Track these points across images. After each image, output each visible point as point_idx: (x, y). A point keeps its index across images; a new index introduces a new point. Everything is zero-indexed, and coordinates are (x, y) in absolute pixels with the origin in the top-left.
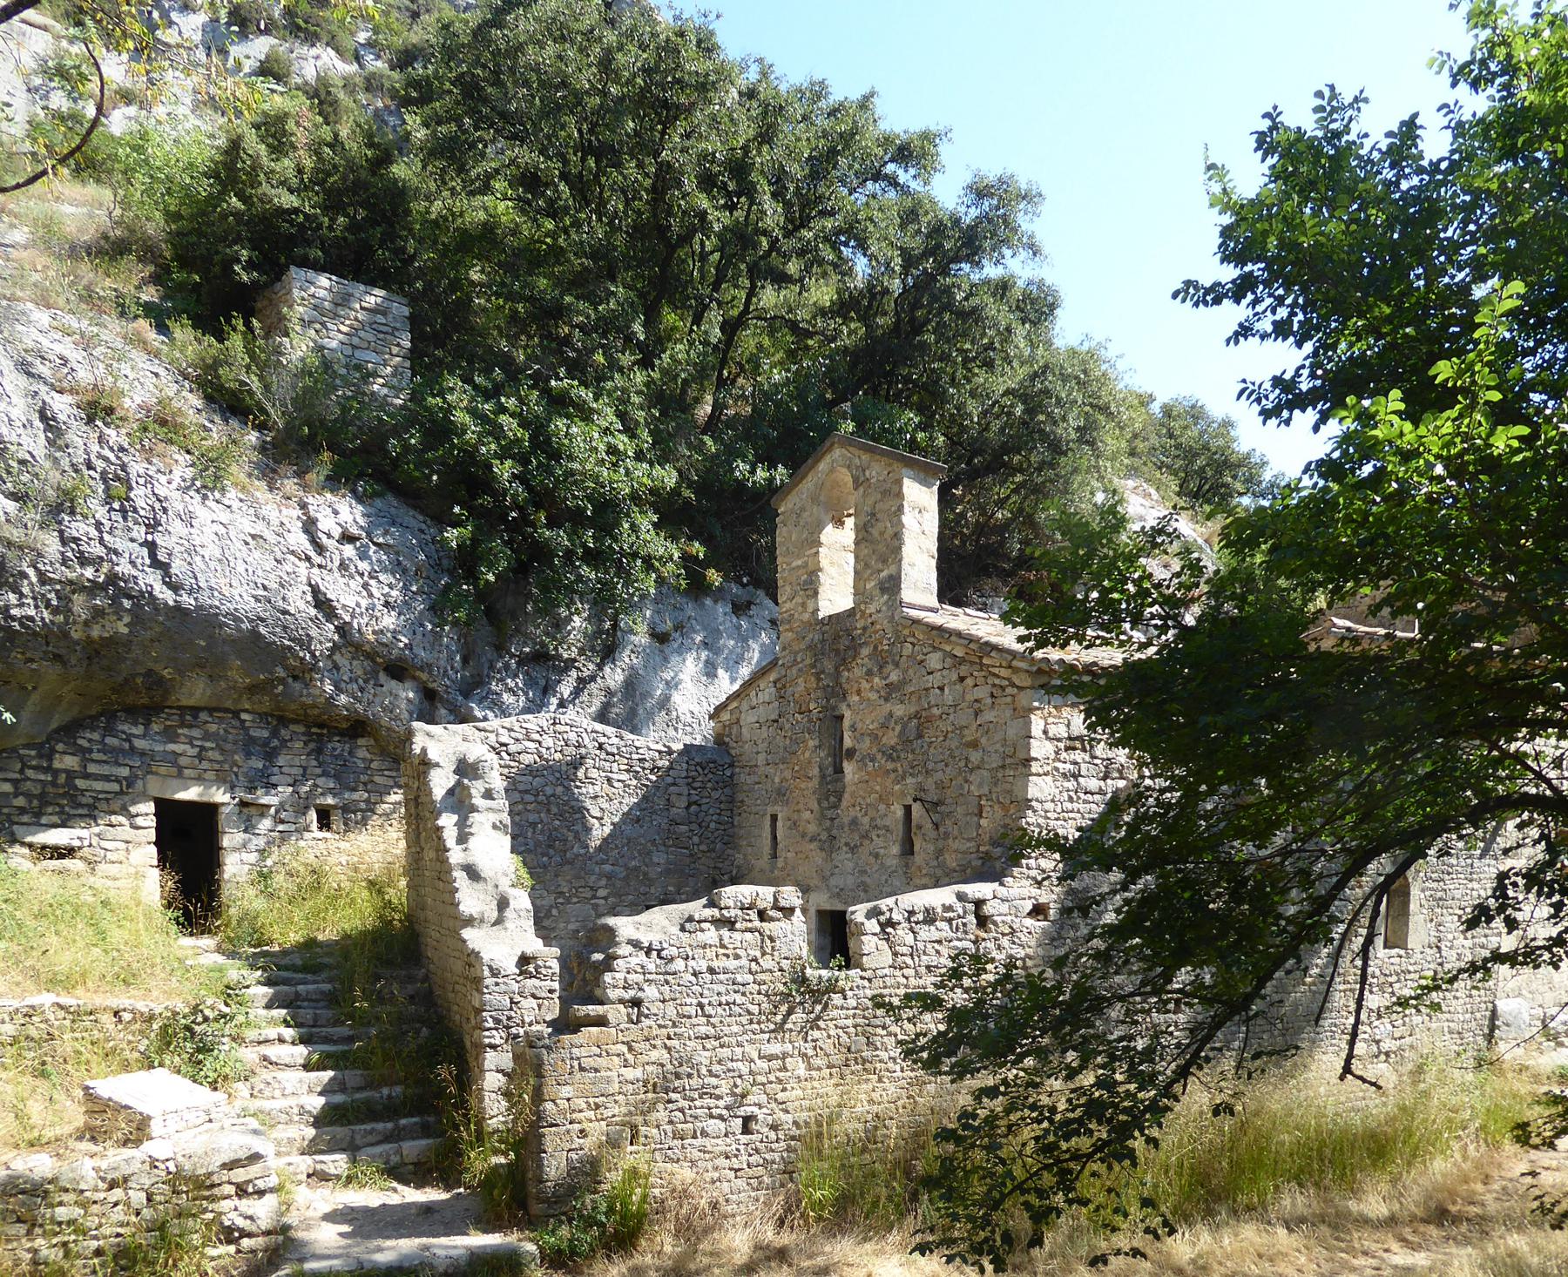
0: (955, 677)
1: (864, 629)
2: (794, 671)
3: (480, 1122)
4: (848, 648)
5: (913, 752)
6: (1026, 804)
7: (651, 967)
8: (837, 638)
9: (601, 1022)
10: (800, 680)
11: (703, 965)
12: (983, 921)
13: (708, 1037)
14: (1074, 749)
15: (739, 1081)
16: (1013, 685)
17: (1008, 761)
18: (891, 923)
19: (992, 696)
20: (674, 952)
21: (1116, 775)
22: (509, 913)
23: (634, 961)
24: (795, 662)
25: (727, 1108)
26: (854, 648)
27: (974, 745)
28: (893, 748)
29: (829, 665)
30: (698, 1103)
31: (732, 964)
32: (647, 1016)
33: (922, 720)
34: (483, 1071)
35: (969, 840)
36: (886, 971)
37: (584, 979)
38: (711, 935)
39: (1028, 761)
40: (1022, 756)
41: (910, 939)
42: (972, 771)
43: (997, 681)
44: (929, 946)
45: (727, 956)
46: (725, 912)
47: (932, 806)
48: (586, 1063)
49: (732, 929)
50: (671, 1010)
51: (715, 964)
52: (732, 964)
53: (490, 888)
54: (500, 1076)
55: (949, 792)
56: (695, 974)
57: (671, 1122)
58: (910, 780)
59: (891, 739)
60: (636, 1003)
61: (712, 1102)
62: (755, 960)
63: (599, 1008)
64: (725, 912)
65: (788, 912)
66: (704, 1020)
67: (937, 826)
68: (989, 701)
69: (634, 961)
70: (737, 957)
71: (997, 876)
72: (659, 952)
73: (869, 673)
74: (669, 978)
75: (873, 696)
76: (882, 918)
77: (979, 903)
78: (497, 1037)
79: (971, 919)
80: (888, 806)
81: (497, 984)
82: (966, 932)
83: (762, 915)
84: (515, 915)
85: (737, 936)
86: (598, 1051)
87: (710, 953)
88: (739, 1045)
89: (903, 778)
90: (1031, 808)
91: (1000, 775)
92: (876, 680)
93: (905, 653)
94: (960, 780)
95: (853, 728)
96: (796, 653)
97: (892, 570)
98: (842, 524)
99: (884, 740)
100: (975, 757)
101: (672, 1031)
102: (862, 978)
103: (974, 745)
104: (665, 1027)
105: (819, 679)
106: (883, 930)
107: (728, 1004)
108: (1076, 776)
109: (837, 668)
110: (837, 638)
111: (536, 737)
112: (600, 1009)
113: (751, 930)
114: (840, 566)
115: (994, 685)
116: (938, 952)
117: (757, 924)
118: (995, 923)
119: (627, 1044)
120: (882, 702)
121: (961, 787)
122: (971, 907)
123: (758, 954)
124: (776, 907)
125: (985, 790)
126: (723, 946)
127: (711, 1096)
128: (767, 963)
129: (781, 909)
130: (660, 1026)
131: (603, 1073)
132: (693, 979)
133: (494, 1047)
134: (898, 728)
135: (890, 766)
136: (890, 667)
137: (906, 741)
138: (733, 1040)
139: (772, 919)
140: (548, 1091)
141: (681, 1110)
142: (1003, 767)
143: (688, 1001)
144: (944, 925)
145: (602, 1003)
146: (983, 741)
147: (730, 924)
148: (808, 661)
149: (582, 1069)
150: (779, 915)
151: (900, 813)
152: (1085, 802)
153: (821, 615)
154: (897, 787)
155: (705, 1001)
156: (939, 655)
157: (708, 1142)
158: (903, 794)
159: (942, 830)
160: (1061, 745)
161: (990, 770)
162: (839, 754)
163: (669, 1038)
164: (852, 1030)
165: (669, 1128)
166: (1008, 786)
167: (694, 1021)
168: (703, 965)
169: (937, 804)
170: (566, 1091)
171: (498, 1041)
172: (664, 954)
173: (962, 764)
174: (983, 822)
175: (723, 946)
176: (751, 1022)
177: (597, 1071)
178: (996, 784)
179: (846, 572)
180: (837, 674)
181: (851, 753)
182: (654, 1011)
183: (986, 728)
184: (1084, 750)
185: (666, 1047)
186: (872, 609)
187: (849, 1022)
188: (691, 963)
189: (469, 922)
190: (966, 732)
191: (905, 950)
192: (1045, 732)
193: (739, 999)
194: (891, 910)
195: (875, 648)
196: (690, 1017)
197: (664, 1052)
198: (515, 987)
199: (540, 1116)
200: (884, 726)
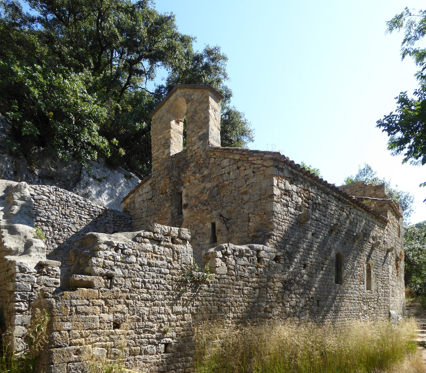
0: (235, 167)
1: (192, 156)
2: (159, 178)
3: (10, 354)
4: (184, 165)
5: (216, 200)
6: (272, 213)
7: (119, 257)
8: (179, 162)
9: (90, 285)
10: (162, 181)
11: (146, 261)
12: (260, 259)
13: (147, 300)
14: (286, 195)
15: (163, 324)
16: (264, 166)
17: (262, 197)
18: (225, 254)
19: (253, 172)
20: (131, 251)
21: (298, 209)
22: (32, 249)
23: (109, 253)
24: (160, 175)
25: (157, 339)
26: (187, 164)
27: (246, 193)
28: (206, 201)
29: (175, 173)
30: (142, 335)
31: (159, 262)
32: (116, 285)
33: (220, 187)
34: (13, 326)
35: (244, 232)
36: (225, 276)
37: (79, 264)
38: (149, 246)
39: (273, 195)
40: (270, 193)
41: (233, 262)
42: (244, 204)
43: (256, 166)
44: (241, 267)
45: (157, 258)
46: (156, 235)
47: (225, 221)
48: (81, 309)
49: (159, 245)
50: (129, 284)
51: (151, 261)
52: (159, 262)
53: (22, 237)
54: (24, 328)
55: (233, 214)
56: (141, 265)
57: (128, 345)
58: (214, 212)
59: (205, 197)
60: (110, 277)
61: (150, 335)
62: (170, 262)
63: (88, 277)
64: (156, 235)
65: (184, 241)
66: (146, 290)
67: (228, 229)
68: (252, 174)
69: (109, 253)
70: (162, 259)
71: (263, 243)
72: (123, 250)
73: (194, 173)
74: (128, 265)
75: (196, 182)
76: (223, 251)
77: (258, 251)
78: (23, 306)
79: (255, 257)
80: (204, 224)
81: (24, 277)
82: (254, 263)
83: (173, 240)
84: (36, 250)
85: (162, 248)
86: (88, 302)
87: (149, 255)
88: (163, 305)
89: (211, 212)
90: (274, 214)
91: (258, 203)
92: (198, 175)
93: (211, 162)
94: (239, 208)
95: (187, 196)
96: (161, 171)
97: (205, 131)
98: (179, 123)
99: (201, 198)
100: (246, 197)
101: (129, 295)
102: (216, 278)
103: (246, 193)
104: (125, 292)
105: (170, 179)
106: (223, 257)
107: (157, 283)
108: (287, 206)
109: (179, 174)
110: (179, 162)
111: (48, 194)
112: (89, 278)
113: (166, 246)
114: (178, 138)
115: (254, 168)
116: (244, 270)
117: (171, 244)
118: (263, 261)
119: (104, 299)
120: (200, 183)
121: (240, 211)
122: (255, 252)
123: (171, 259)
124: (179, 237)
125: (252, 210)
126: (155, 253)
127: (149, 332)
128: (176, 265)
129: (182, 239)
130: (123, 292)
131: (90, 316)
132: (140, 267)
133: (21, 312)
134: (208, 193)
135: (205, 208)
136: (204, 169)
137: (212, 197)
138: (160, 303)
139: (177, 243)
140: (57, 324)
141: (134, 339)
142: (260, 200)
143: (138, 279)
144: (245, 258)
145: (90, 275)
146: (250, 191)
147: (158, 241)
148: (166, 173)
149: (77, 312)
150: (181, 241)
151: (209, 226)
152: (290, 217)
153: (171, 155)
154: (208, 216)
155: (147, 280)
156: (227, 160)
157: (148, 357)
158: (211, 218)
159: (230, 230)
160: (283, 192)
161: (254, 202)
162: (180, 207)
163: (128, 299)
164: (212, 302)
165: (127, 349)
166: (263, 207)
167: (141, 290)
168: (146, 261)
169: (228, 220)
170: (67, 325)
171: (23, 308)
172: (126, 251)
173: (240, 201)
174: (251, 224)
175: (155, 253)
176: (168, 294)
177: (86, 314)
178: (257, 207)
179: (180, 142)
180: (179, 174)
181: (186, 206)
182: (120, 282)
183: (251, 186)
184: (289, 196)
185: (126, 303)
186: (195, 147)
187: (211, 298)
188: (140, 259)
189: (10, 252)
190: (241, 189)
191: (232, 267)
192: (278, 185)
193: (163, 281)
194: (226, 248)
195: (197, 162)
196: (138, 288)
197: (125, 306)
198: (36, 279)
199: (51, 340)
200: (202, 193)
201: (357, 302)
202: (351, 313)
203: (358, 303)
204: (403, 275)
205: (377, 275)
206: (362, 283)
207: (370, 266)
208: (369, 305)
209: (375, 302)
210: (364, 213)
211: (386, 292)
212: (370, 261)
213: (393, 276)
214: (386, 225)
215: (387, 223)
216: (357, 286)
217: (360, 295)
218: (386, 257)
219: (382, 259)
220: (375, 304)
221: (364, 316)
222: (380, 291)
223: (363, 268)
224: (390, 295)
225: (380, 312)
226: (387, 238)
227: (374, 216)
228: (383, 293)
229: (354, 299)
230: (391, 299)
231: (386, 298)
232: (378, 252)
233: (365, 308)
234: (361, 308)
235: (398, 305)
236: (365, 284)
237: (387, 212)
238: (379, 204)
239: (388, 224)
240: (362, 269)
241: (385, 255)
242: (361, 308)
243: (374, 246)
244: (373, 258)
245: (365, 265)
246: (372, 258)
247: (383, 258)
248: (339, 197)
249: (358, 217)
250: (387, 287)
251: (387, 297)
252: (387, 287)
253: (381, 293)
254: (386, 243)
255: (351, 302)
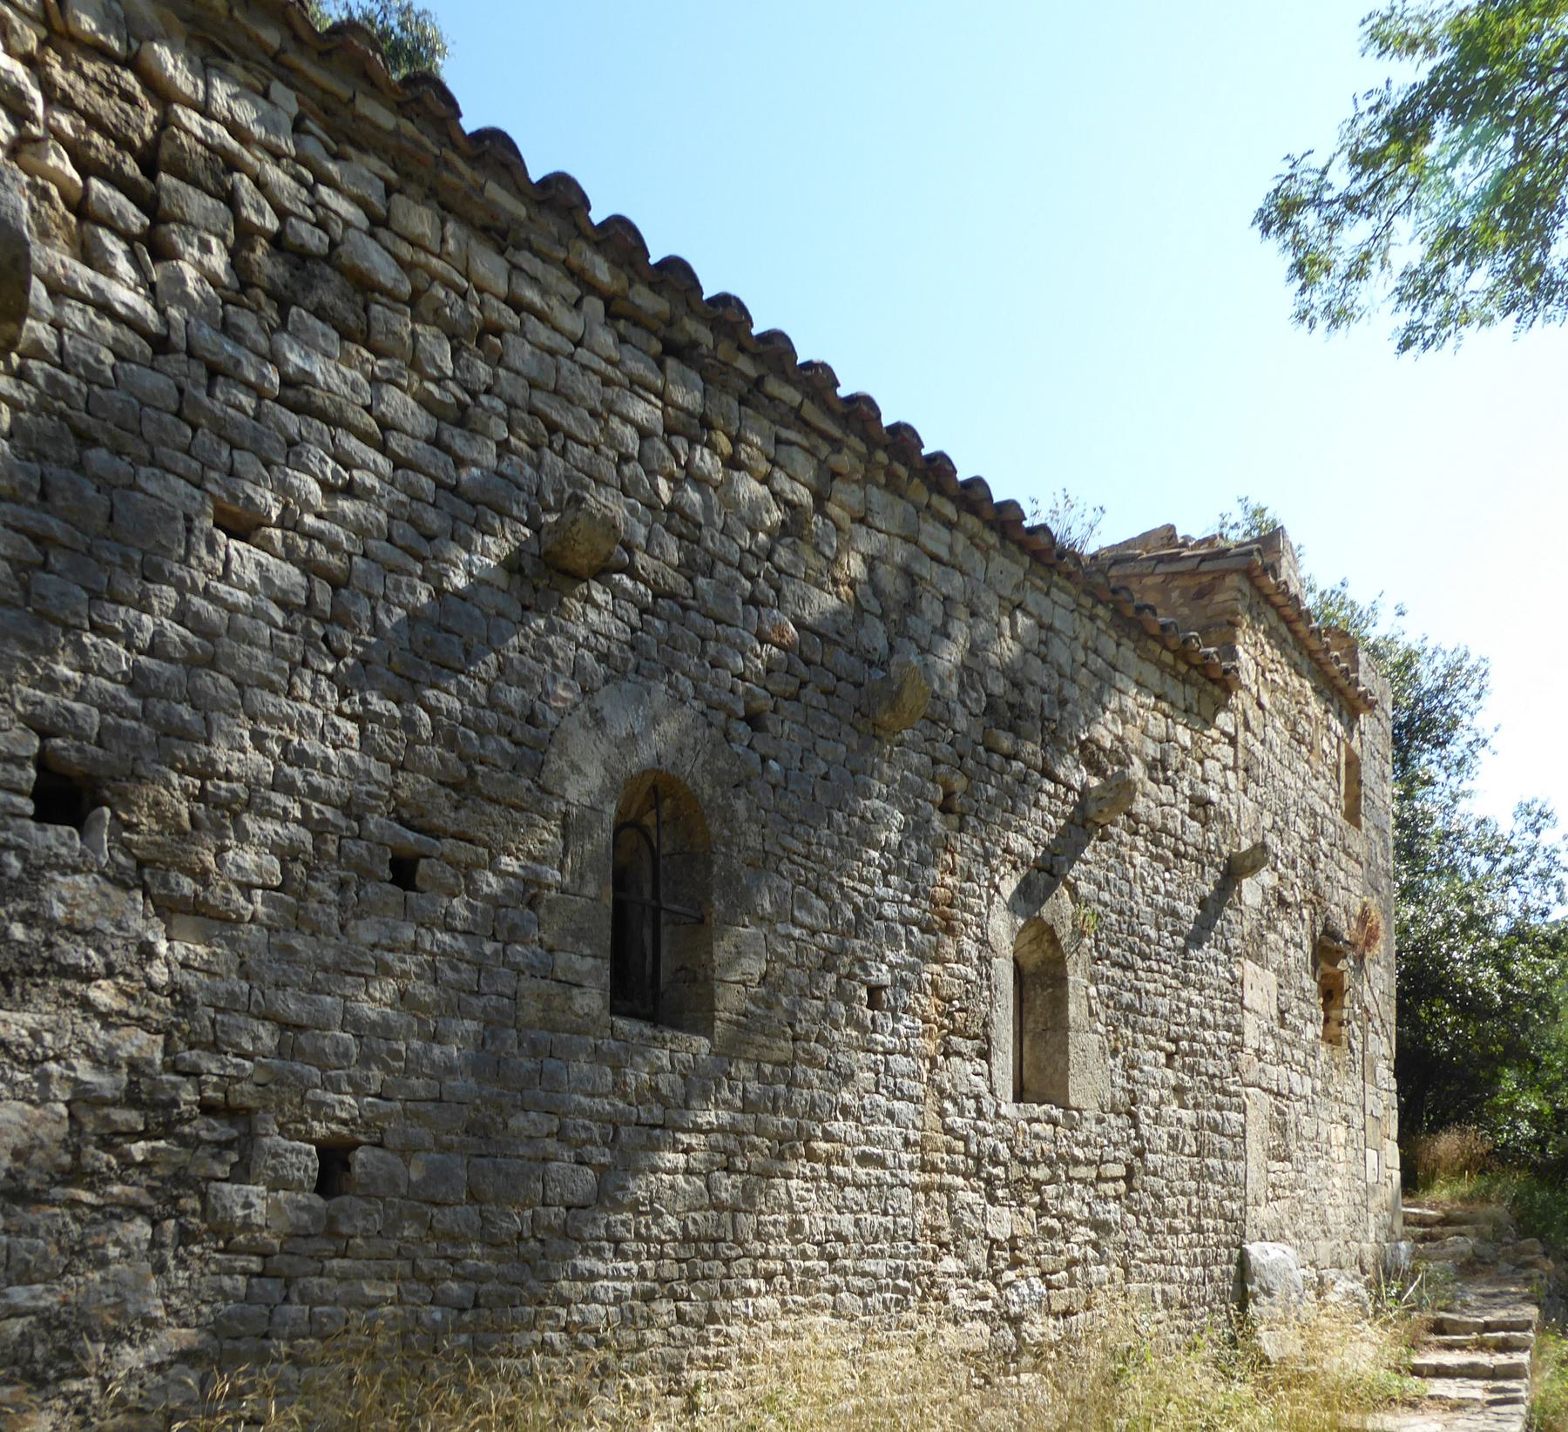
201: (916, 1177)
202: (832, 1258)
203: (926, 1189)
204: (1383, 1047)
205: (1130, 1007)
206: (966, 1046)
207: (1055, 941)
208: (1042, 1208)
209: (1108, 1188)
210: (999, 561)
211: (1215, 1128)
212: (1060, 908)
213: (1286, 1034)
214: (1220, 705)
215: (1228, 691)
216: (900, 1063)
217: (949, 1130)
218: (1213, 907)
219: (1174, 913)
220: (1104, 1199)
221: (994, 1277)
222: (1157, 1120)
223: (983, 942)
224: (1255, 1149)
225: (1152, 1252)
226: (1225, 789)
227: (1100, 610)
228: (1189, 1135)
229: (864, 1159)
230: (1256, 1168)
231: (1212, 1162)
232: (1139, 860)
233: (1003, 1222)
234: (957, 1223)
235: (1338, 1217)
236: (1004, 1062)
237: (1233, 625)
238: (1191, 583)
239: (1240, 700)
240: (970, 947)
241: (1208, 889)
242: (957, 1223)
243: (1092, 810)
244: (1084, 888)
245: (1002, 927)
246: (1073, 889)
247: (1190, 911)
248: (670, 323)
249: (926, 569)
250: (1225, 1092)
251: (1223, 1155)
252: (1225, 1092)
253: (1163, 1131)
254: (1222, 817)
255: (830, 1177)
